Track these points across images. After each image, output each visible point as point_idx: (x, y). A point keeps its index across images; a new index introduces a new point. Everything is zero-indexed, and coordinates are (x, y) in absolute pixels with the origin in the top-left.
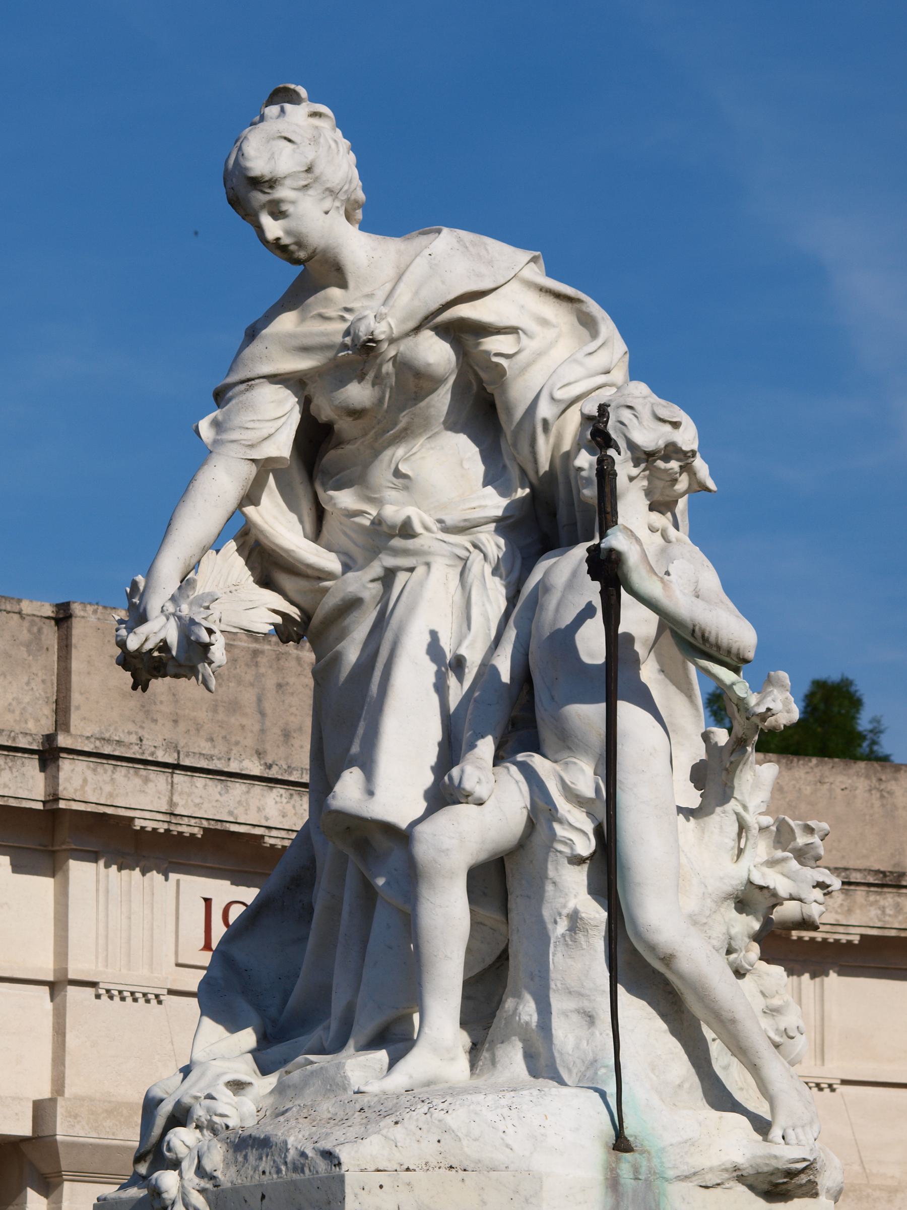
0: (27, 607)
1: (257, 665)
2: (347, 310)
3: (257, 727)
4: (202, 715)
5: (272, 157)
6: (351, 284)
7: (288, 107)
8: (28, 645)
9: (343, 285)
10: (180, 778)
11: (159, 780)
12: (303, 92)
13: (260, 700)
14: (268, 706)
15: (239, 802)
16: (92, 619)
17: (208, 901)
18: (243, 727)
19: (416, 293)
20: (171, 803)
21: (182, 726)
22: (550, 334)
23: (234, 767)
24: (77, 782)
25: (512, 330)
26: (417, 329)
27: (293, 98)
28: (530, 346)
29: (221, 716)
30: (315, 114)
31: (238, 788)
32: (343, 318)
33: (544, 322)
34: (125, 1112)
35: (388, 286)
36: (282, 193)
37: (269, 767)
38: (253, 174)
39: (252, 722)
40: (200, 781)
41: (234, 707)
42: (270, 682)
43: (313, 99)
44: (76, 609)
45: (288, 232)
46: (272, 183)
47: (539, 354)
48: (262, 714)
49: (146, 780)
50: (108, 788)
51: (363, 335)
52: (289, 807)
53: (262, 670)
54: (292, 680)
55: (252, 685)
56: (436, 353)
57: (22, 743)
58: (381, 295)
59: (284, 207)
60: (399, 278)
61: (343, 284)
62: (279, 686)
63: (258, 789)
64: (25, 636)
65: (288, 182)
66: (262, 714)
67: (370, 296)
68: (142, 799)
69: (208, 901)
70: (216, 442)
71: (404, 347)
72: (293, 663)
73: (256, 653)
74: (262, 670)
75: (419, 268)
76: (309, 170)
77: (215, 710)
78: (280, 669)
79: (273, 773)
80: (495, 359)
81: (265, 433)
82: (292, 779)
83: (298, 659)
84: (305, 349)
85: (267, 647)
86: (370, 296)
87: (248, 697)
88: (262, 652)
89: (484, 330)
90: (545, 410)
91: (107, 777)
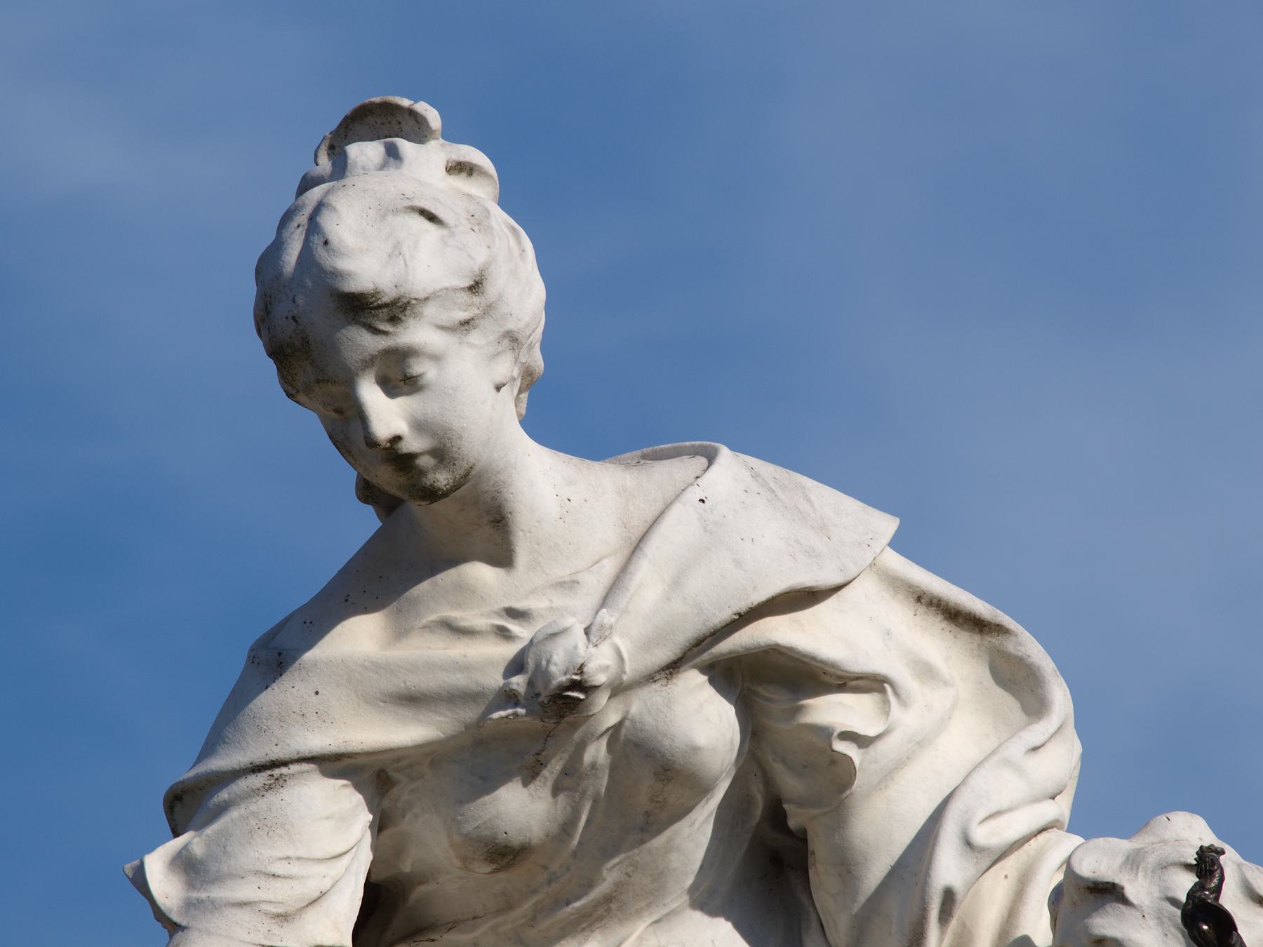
2: (513, 614)
5: (396, 251)
6: (522, 556)
7: (404, 145)
9: (502, 557)
12: (433, 117)
19: (676, 583)
22: (940, 699)
25: (873, 683)
26: (672, 668)
27: (418, 130)
28: (908, 720)
30: (460, 168)
32: (504, 634)
33: (926, 672)
35: (609, 567)
36: (417, 334)
38: (353, 286)
43: (451, 135)
45: (420, 426)
46: (397, 310)
47: (921, 743)
51: (559, 676)
56: (704, 722)
58: (595, 583)
59: (416, 367)
60: (637, 546)
61: (502, 557)
65: (430, 311)
67: (569, 585)
70: (190, 905)
71: (641, 705)
75: (678, 530)
76: (476, 287)
80: (840, 746)
81: (312, 887)
84: (412, 700)
86: (569, 585)
89: (810, 677)
90: (949, 868)
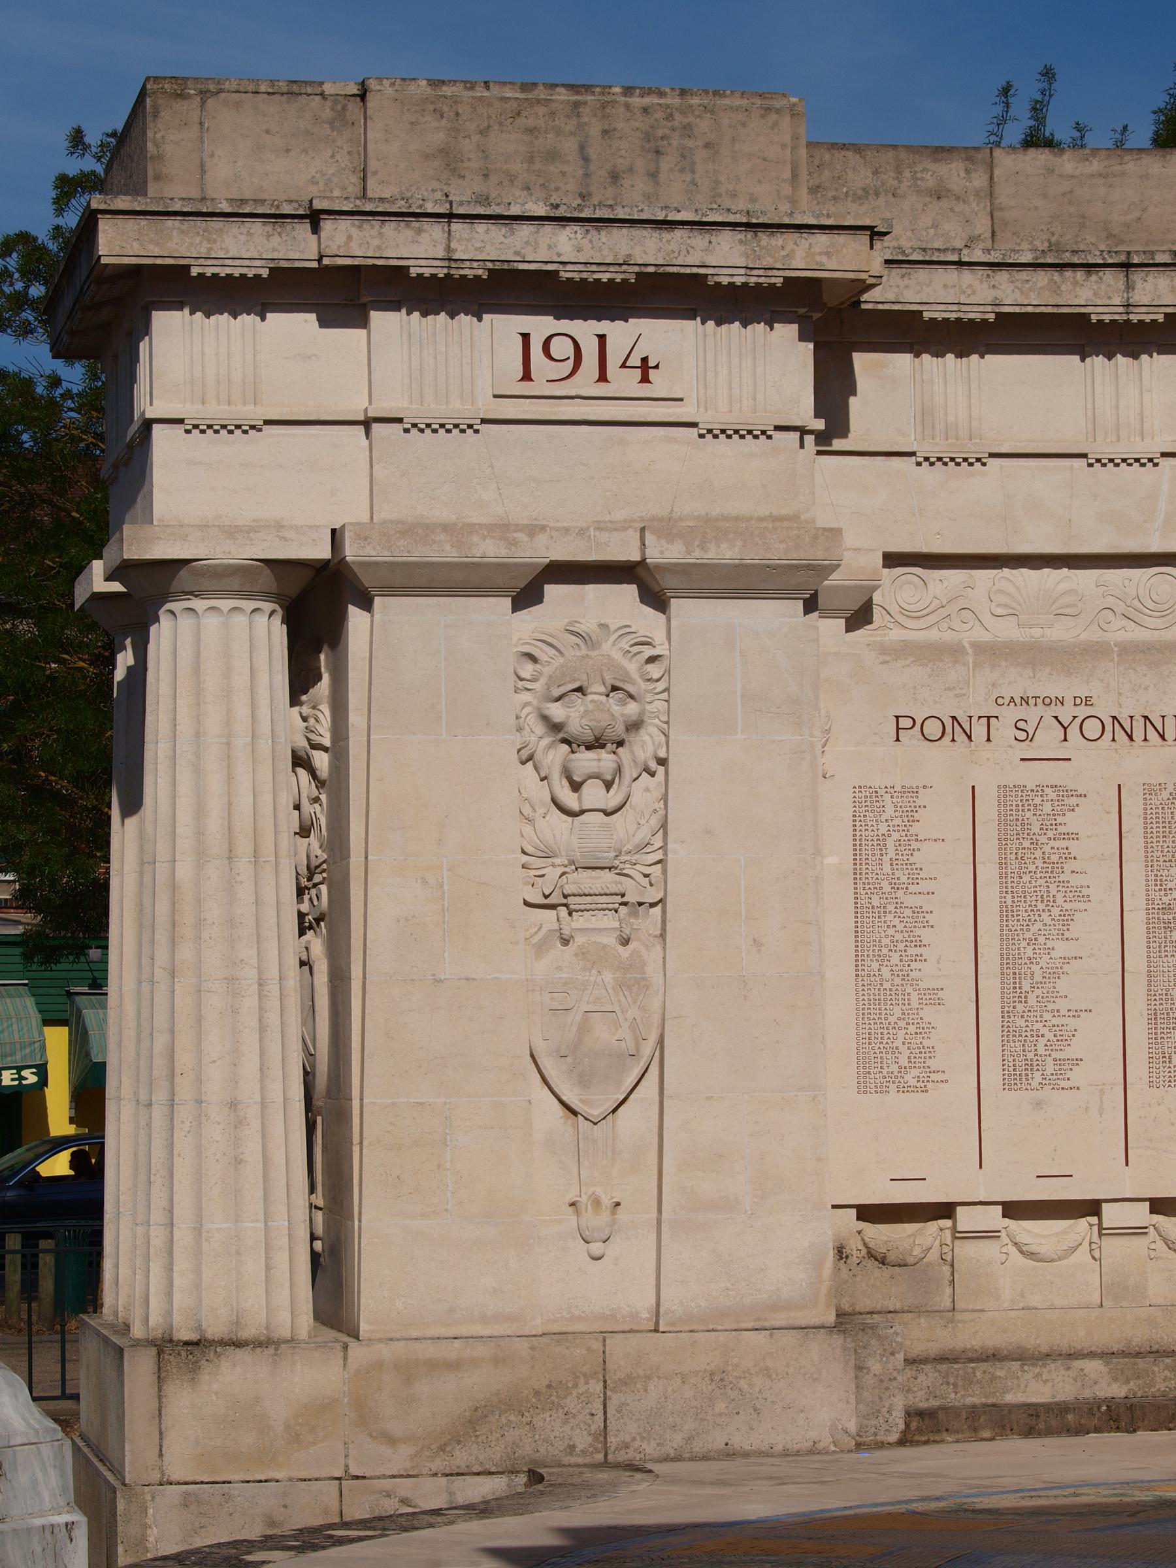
0: (328, 88)
1: (578, 115)
3: (580, 172)
4: (516, 167)
8: (331, 122)
10: (457, 226)
11: (436, 231)
13: (582, 148)
14: (592, 152)
15: (527, 243)
16: (390, 91)
17: (526, 337)
18: (563, 174)
20: (448, 248)
21: (494, 179)
23: (515, 210)
24: (340, 239)
29: (538, 166)
31: (525, 231)
34: (420, 531)
37: (557, 206)
39: (574, 168)
40: (481, 227)
41: (553, 156)
42: (595, 129)
44: (372, 84)
48: (586, 159)
49: (419, 231)
50: (376, 242)
52: (585, 242)
53: (585, 119)
54: (620, 125)
55: (573, 134)
57: (287, 209)
62: (605, 132)
63: (548, 229)
64: (328, 113)
66: (586, 159)
68: (419, 249)
69: (526, 337)
72: (621, 110)
73: (577, 105)
74: (585, 119)
77: (531, 160)
78: (606, 117)
79: (561, 212)
82: (583, 215)
83: (627, 106)
85: (590, 98)
87: (569, 146)
88: (585, 103)
91: (374, 232)
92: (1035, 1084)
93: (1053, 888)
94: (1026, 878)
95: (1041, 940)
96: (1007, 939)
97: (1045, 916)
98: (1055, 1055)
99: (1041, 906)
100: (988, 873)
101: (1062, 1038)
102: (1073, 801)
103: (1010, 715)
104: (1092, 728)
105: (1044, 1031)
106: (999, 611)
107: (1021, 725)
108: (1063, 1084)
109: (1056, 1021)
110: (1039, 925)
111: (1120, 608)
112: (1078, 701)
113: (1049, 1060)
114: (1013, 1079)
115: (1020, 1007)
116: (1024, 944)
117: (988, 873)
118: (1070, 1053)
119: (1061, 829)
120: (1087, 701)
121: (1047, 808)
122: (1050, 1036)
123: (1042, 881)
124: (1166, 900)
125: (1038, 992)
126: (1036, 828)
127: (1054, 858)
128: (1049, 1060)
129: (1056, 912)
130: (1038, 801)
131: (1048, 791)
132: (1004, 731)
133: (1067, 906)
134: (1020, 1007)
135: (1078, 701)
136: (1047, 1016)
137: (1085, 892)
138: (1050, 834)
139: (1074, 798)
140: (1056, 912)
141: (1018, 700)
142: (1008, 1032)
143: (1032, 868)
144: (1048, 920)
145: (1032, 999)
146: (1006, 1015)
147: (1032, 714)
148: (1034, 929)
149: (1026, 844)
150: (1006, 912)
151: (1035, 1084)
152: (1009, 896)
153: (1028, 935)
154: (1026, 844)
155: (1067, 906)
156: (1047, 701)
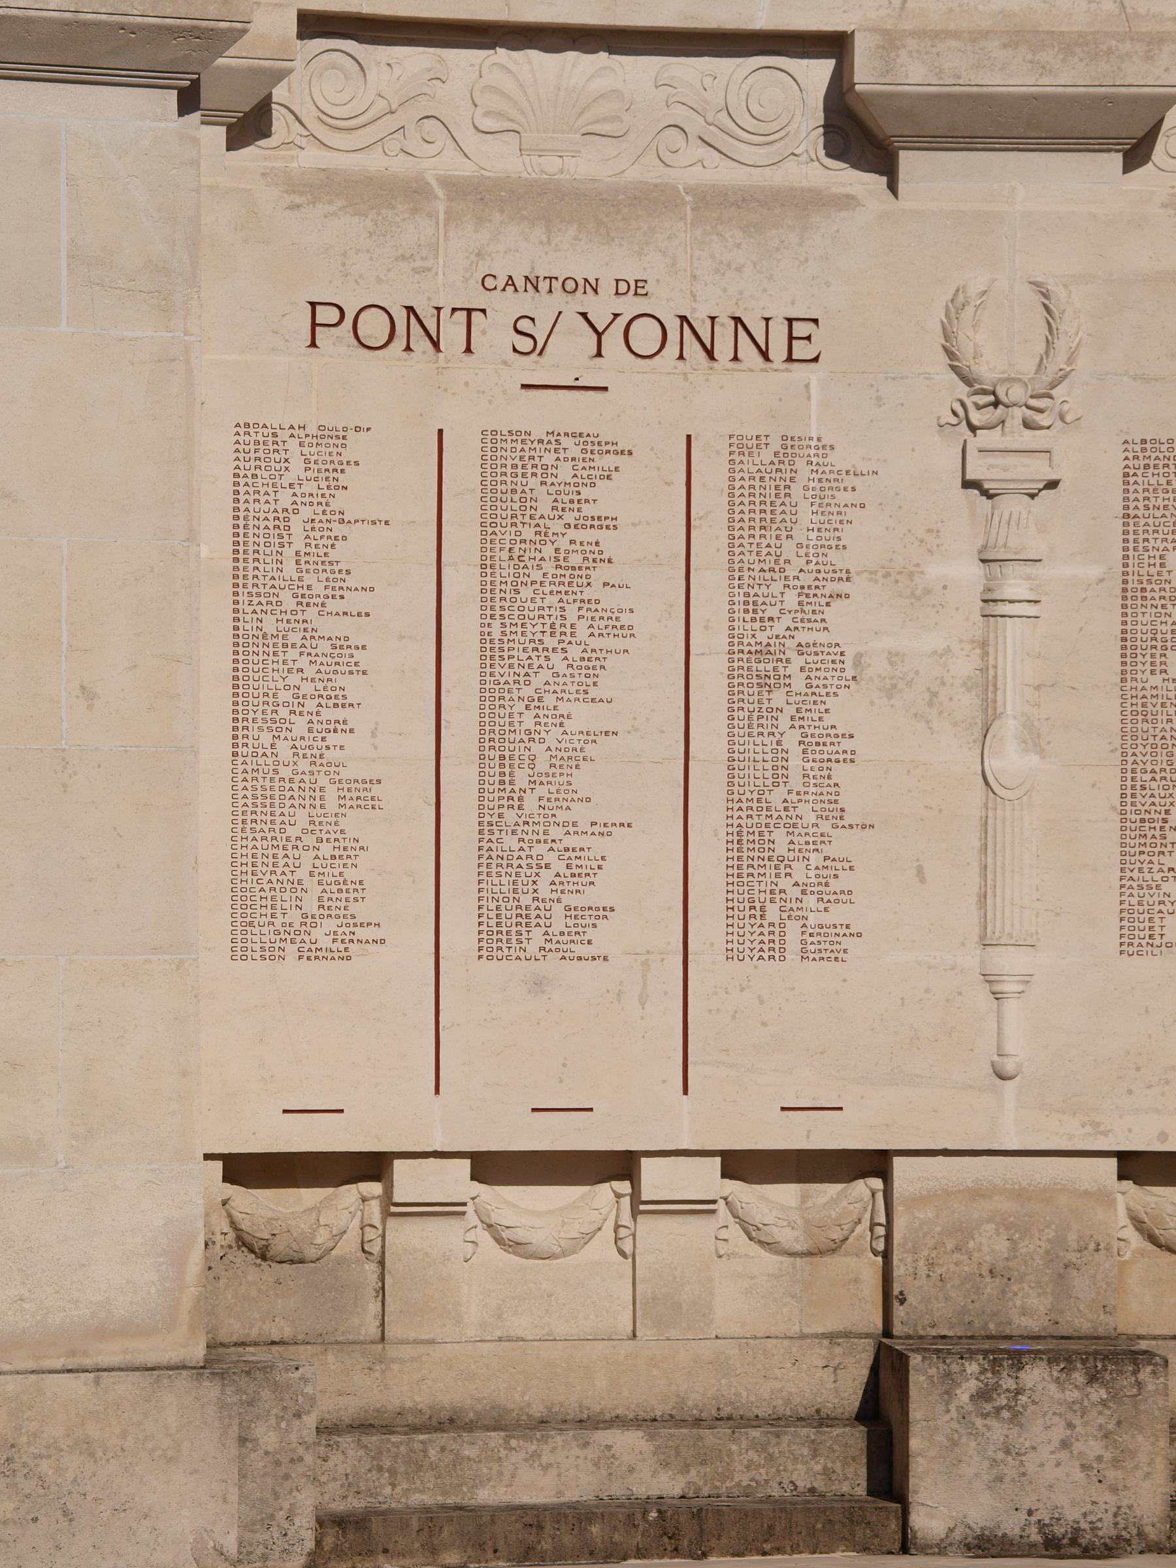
92: (532, 949)
93: (572, 612)
94: (526, 593)
95: (550, 700)
96: (492, 697)
97: (556, 658)
98: (568, 899)
99: (550, 642)
100: (462, 581)
101: (581, 872)
102: (609, 461)
103: (505, 307)
104: (645, 336)
105: (551, 858)
106: (488, 124)
107: (524, 325)
108: (580, 950)
109: (570, 841)
110: (546, 675)
111: (695, 125)
112: (623, 287)
113: (558, 909)
114: (496, 941)
115: (510, 816)
116: (520, 707)
117: (462, 581)
118: (591, 897)
119: (588, 510)
120: (638, 288)
121: (565, 472)
122: (560, 867)
123: (553, 600)
124: (762, 637)
125: (541, 791)
126: (544, 508)
127: (575, 560)
128: (558, 909)
129: (575, 652)
130: (549, 459)
131: (566, 442)
132: (495, 335)
133: (595, 643)
134: (510, 816)
135: (623, 287)
136: (555, 832)
137: (625, 619)
138: (569, 517)
139: (611, 457)
140: (575, 652)
141: (520, 282)
142: (488, 857)
143: (537, 575)
144: (561, 667)
145: (531, 803)
146: (485, 829)
147: (544, 307)
148: (537, 681)
149: (528, 533)
150: (490, 651)
151: (532, 949)
152: (496, 624)
153: (527, 692)
154: (528, 533)
155: (595, 643)
156: (570, 285)
